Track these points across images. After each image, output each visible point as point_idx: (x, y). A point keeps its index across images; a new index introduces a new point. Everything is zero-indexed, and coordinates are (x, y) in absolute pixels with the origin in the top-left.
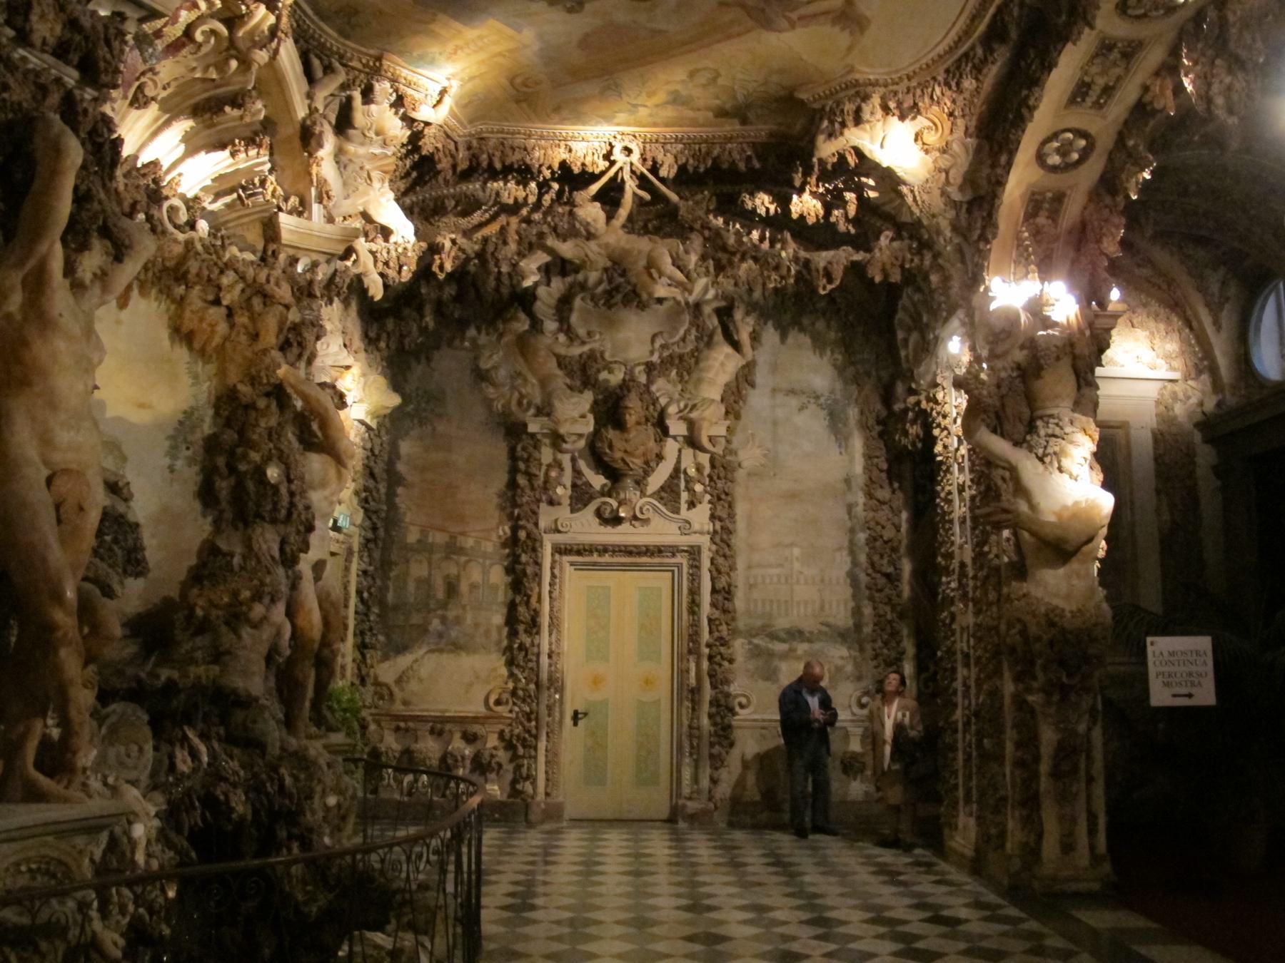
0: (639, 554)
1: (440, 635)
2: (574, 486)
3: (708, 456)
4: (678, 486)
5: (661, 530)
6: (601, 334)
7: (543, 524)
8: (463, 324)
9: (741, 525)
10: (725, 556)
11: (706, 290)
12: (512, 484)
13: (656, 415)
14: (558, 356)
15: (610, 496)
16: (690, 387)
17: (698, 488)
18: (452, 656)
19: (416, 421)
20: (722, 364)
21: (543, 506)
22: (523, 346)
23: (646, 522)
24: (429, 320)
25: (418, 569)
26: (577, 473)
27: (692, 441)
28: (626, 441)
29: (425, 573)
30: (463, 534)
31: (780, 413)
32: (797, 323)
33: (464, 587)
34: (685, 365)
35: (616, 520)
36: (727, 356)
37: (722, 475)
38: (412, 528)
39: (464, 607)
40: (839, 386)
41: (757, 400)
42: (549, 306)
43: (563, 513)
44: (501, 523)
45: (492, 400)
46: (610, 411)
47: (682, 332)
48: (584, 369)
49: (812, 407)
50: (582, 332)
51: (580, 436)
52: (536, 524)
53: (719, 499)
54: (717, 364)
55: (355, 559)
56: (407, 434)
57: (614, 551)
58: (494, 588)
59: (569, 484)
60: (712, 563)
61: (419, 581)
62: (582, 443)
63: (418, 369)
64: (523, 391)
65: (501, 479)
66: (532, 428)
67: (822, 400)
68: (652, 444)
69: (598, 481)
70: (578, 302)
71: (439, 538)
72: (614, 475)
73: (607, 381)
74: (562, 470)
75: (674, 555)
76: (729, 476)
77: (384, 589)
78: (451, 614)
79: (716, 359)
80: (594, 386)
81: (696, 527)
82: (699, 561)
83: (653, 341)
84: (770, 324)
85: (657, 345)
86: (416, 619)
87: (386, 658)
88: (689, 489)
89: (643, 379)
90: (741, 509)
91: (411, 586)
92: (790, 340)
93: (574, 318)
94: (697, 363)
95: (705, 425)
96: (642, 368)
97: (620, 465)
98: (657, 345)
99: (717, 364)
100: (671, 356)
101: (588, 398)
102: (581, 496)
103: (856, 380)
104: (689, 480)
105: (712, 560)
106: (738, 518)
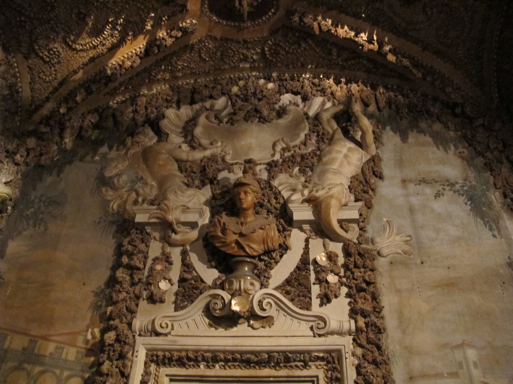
0: (260, 364)
2: (182, 280)
3: (341, 245)
4: (307, 278)
5: (288, 332)
6: (222, 142)
7: (138, 323)
8: (97, 144)
9: (390, 321)
10: (374, 362)
11: (323, 104)
12: (112, 282)
13: (278, 206)
14: (178, 161)
15: (223, 289)
16: (315, 179)
17: (332, 278)
19: (31, 222)
20: (346, 156)
21: (143, 304)
22: (147, 155)
23: (268, 321)
24: (68, 142)
26: (187, 266)
27: (321, 229)
28: (242, 224)
30: (45, 338)
31: (414, 200)
32: (414, 126)
34: (309, 164)
35: (230, 319)
36: (350, 150)
37: (360, 262)
40: (471, 174)
41: (388, 189)
42: (177, 126)
43: (163, 314)
44: (91, 325)
45: (109, 201)
46: (227, 202)
47: (302, 136)
48: (203, 170)
49: (448, 194)
50: (205, 142)
51: (193, 225)
52: (130, 325)
53: (361, 290)
54: (340, 156)
56: (20, 233)
57: (226, 361)
59: (175, 279)
60: (359, 373)
62: (194, 234)
63: (49, 180)
64: (141, 191)
65: (102, 275)
66: (140, 218)
67: (457, 187)
68: (274, 233)
69: (210, 275)
70: (202, 119)
72: (227, 263)
73: (227, 179)
74: (171, 263)
75: (306, 366)
76: (368, 263)
79: (339, 152)
80: (211, 183)
81: (333, 325)
82: (341, 372)
83: (274, 145)
84: (388, 128)
85: (279, 148)
88: (321, 281)
89: (265, 176)
90: (388, 301)
92: (411, 140)
93: (198, 131)
94: (320, 159)
95: (334, 203)
96: (263, 167)
97: (234, 250)
98: (279, 148)
99: (340, 156)
100: (293, 156)
101: (206, 193)
102: (189, 290)
103: (489, 167)
104: (320, 270)
105: (358, 368)
106: (385, 312)
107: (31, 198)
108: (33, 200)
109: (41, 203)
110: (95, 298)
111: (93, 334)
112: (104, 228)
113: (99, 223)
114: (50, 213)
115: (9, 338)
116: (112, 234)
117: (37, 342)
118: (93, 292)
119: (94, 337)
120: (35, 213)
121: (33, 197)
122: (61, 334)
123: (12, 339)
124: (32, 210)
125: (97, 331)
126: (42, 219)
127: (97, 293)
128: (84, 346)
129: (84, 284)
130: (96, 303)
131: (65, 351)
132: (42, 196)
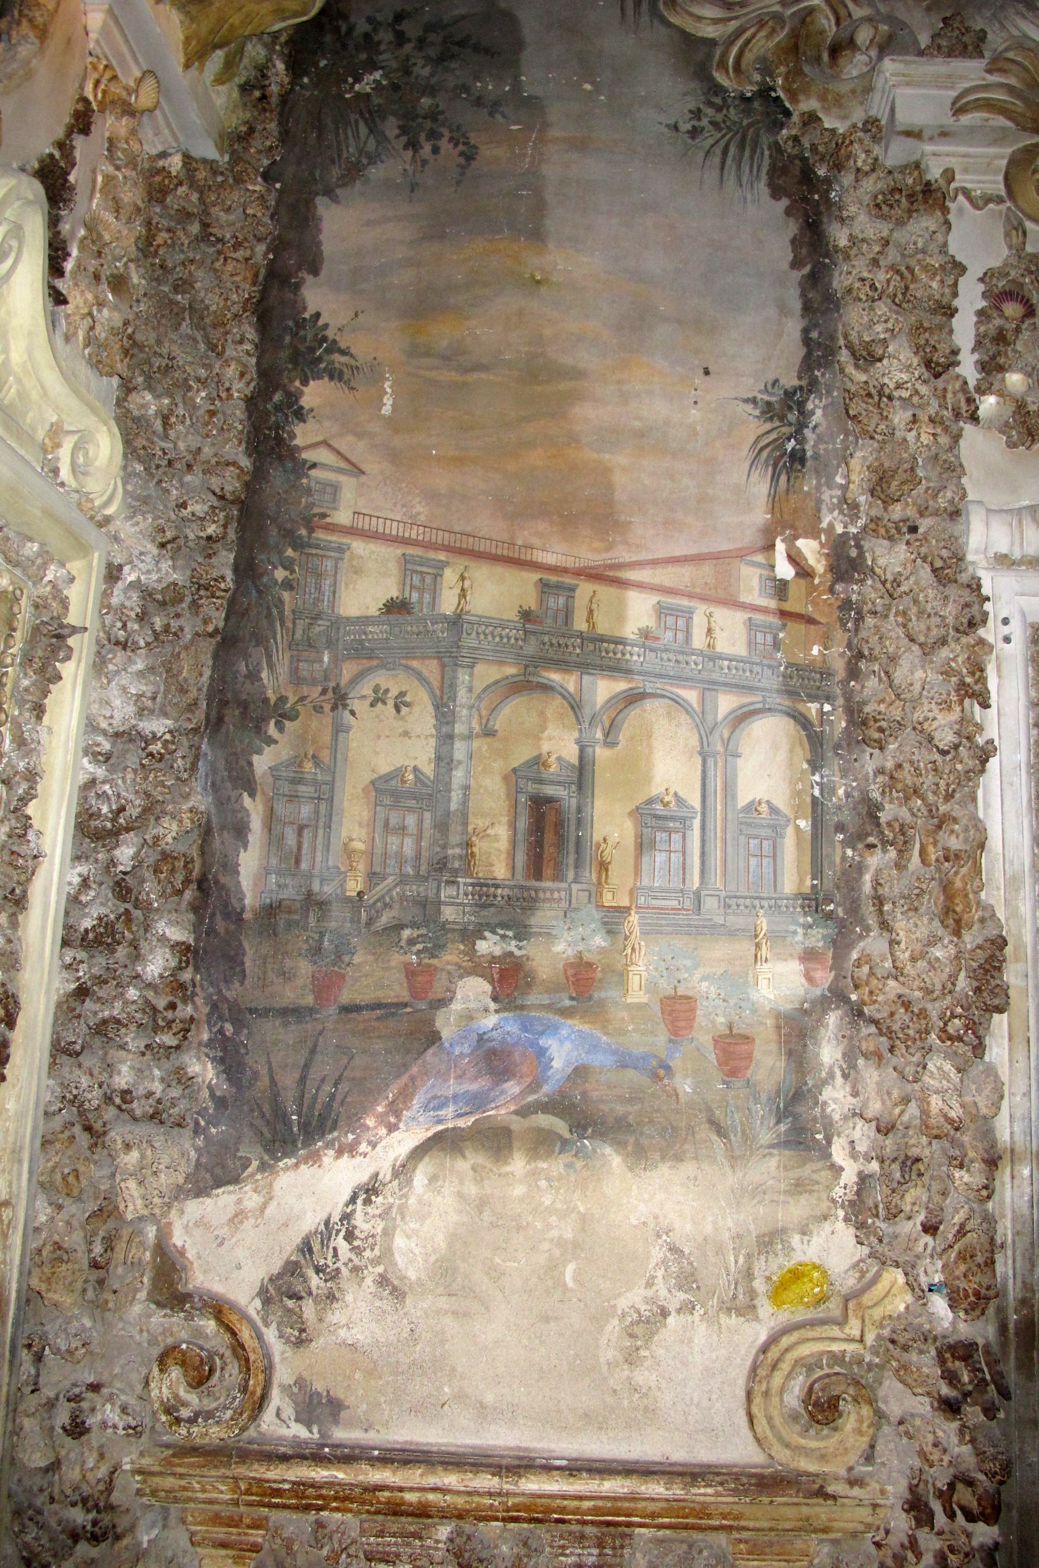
1: (495, 1060)
18: (555, 1166)
19: (391, 127)
25: (386, 741)
29: (419, 755)
33: (610, 824)
38: (359, 547)
39: (613, 921)
55: (73, 671)
56: (354, 172)
58: (758, 824)
61: (388, 790)
71: (495, 595)
77: (217, 831)
78: (560, 941)
86: (374, 975)
87: (215, 1173)
91: (353, 822)
107: (351, 29)
108: (367, 36)
109: (408, 48)
110: (768, 426)
111: (794, 558)
112: (725, 152)
113: (694, 132)
114: (465, 88)
115: (450, 576)
116: (764, 178)
117: (572, 589)
118: (754, 401)
119: (804, 572)
120: (395, 87)
121: (362, 26)
122: (654, 563)
123: (462, 578)
124: (377, 75)
125: (809, 548)
126: (433, 115)
127: (769, 404)
128: (772, 604)
129: (707, 372)
130: (778, 444)
131: (699, 622)
132: (399, 17)
